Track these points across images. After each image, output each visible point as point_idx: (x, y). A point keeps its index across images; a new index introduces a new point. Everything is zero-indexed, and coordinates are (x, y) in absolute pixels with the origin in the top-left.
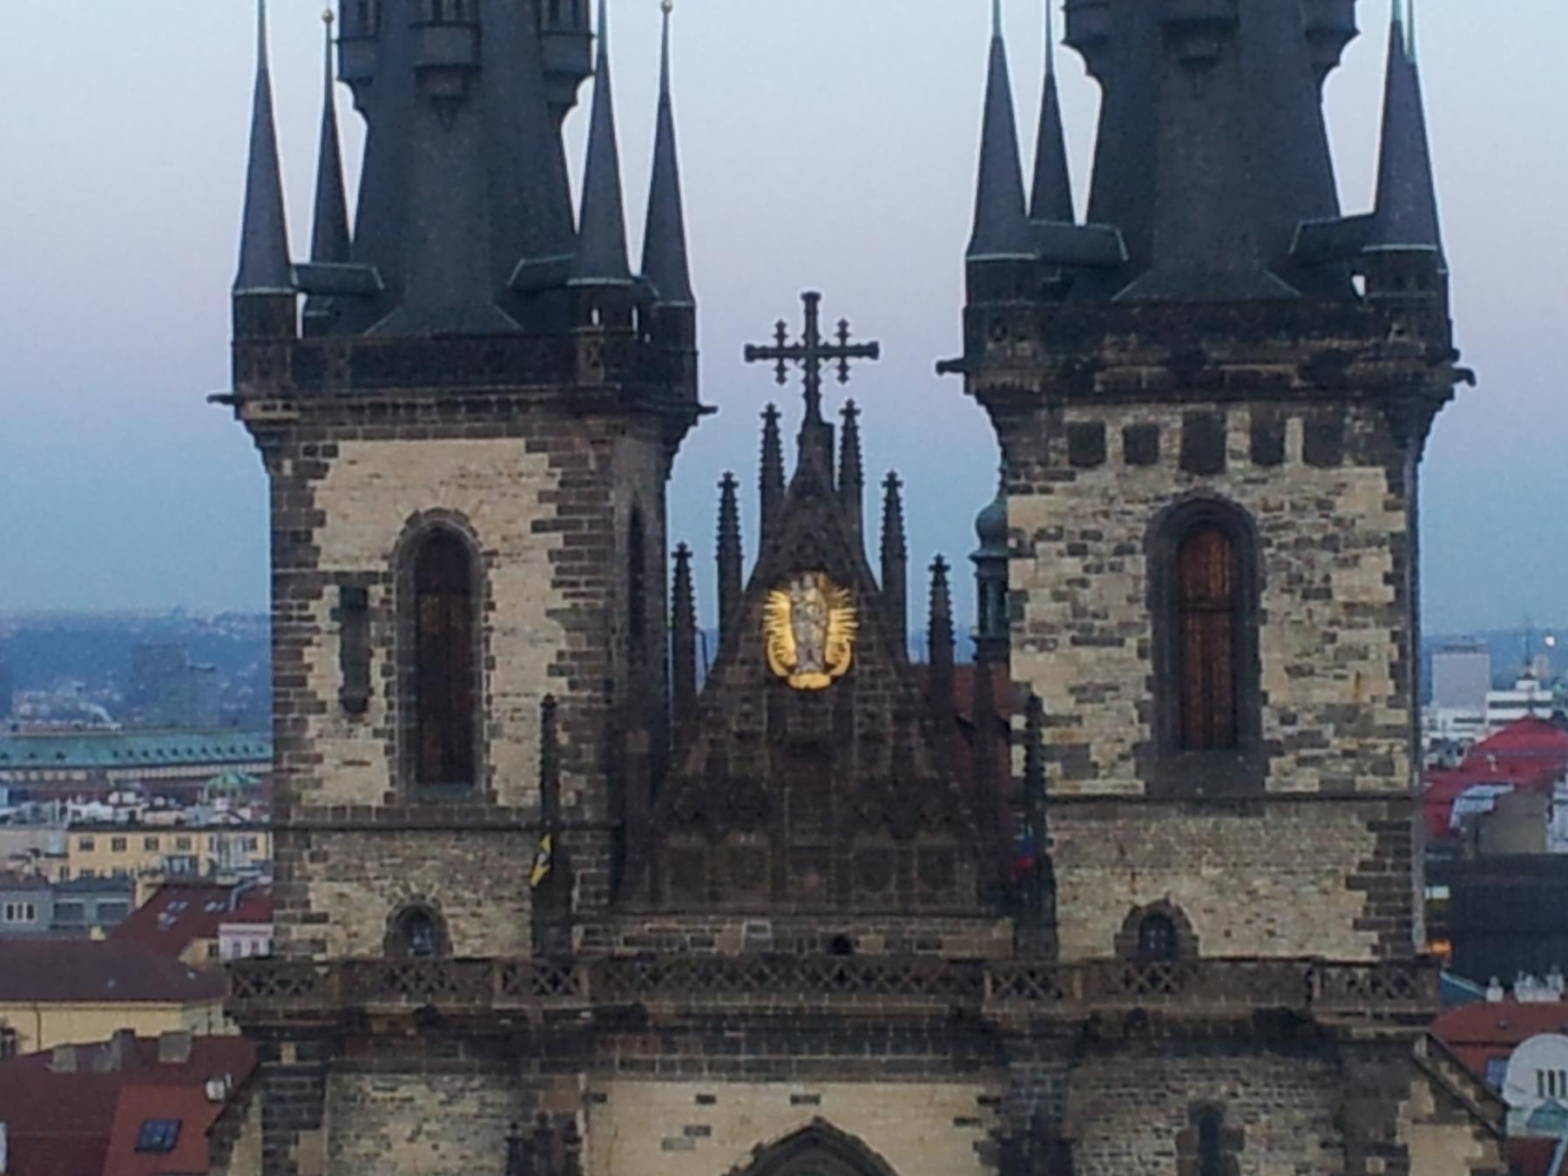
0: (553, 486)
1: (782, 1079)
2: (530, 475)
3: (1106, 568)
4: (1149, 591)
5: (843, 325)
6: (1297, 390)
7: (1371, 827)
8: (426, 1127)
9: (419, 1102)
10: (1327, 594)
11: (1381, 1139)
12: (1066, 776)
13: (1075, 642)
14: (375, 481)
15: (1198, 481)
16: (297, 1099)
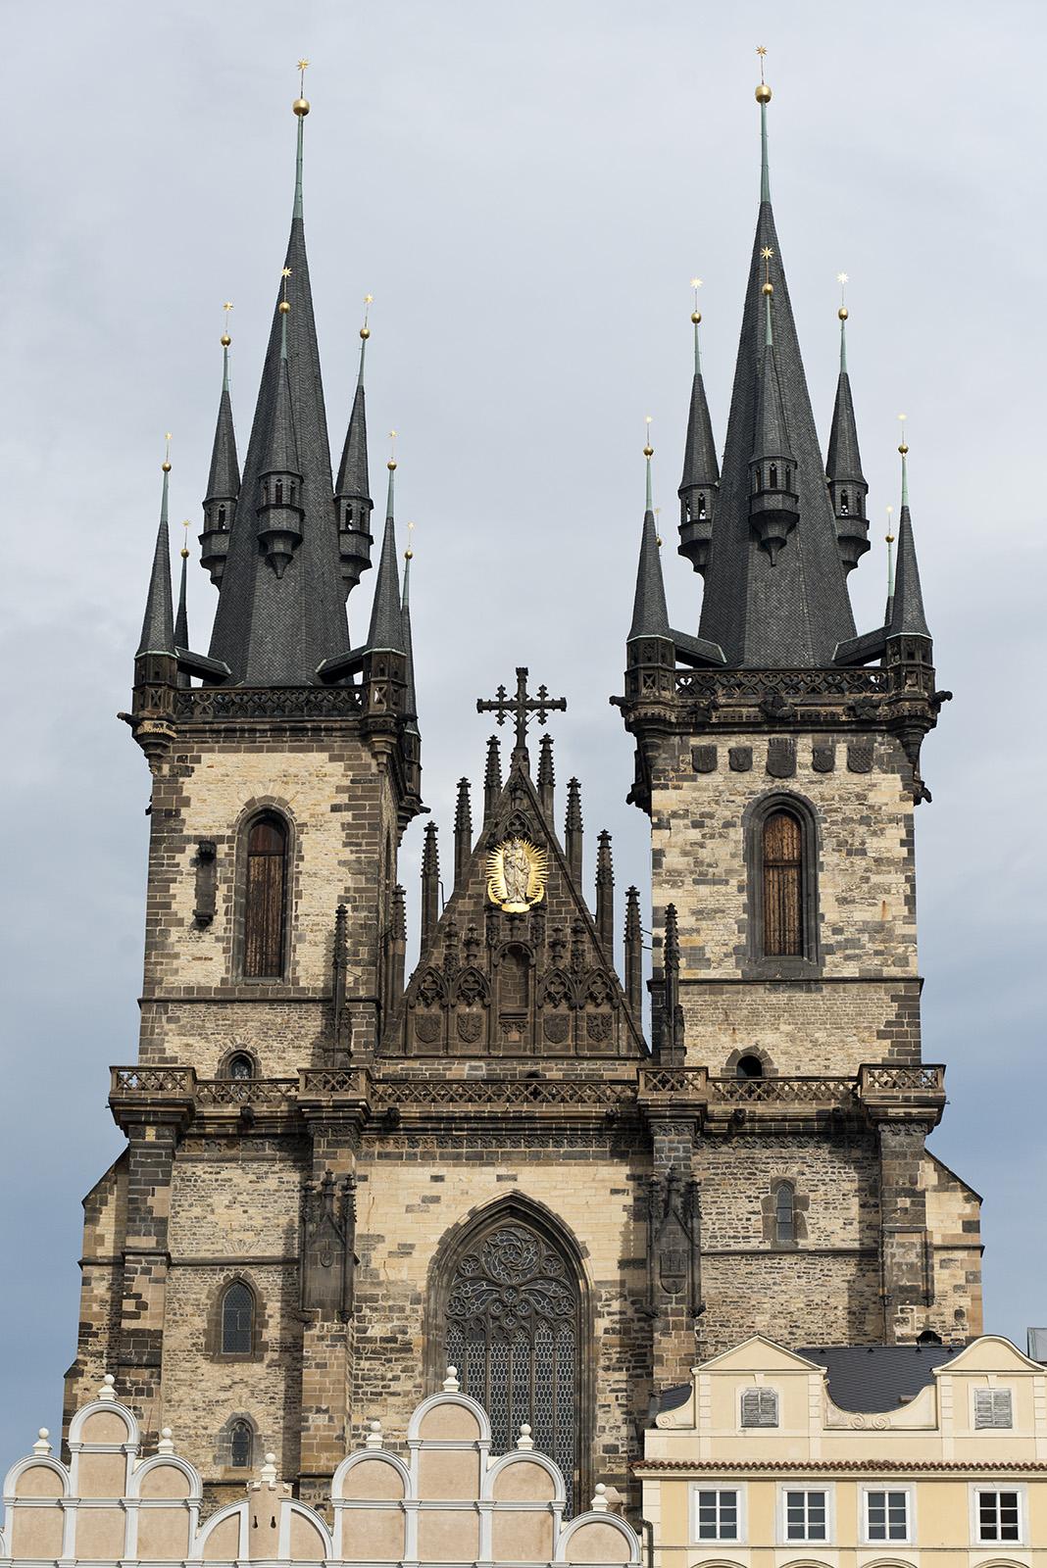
0: (347, 782)
1: (493, 1164)
2: (331, 776)
3: (717, 836)
4: (746, 852)
5: (543, 688)
6: (844, 723)
7: (894, 999)
8: (240, 1198)
10: (863, 852)
11: (907, 1185)
12: (689, 967)
13: (696, 882)
14: (226, 778)
15: (778, 782)
16: (158, 1164)
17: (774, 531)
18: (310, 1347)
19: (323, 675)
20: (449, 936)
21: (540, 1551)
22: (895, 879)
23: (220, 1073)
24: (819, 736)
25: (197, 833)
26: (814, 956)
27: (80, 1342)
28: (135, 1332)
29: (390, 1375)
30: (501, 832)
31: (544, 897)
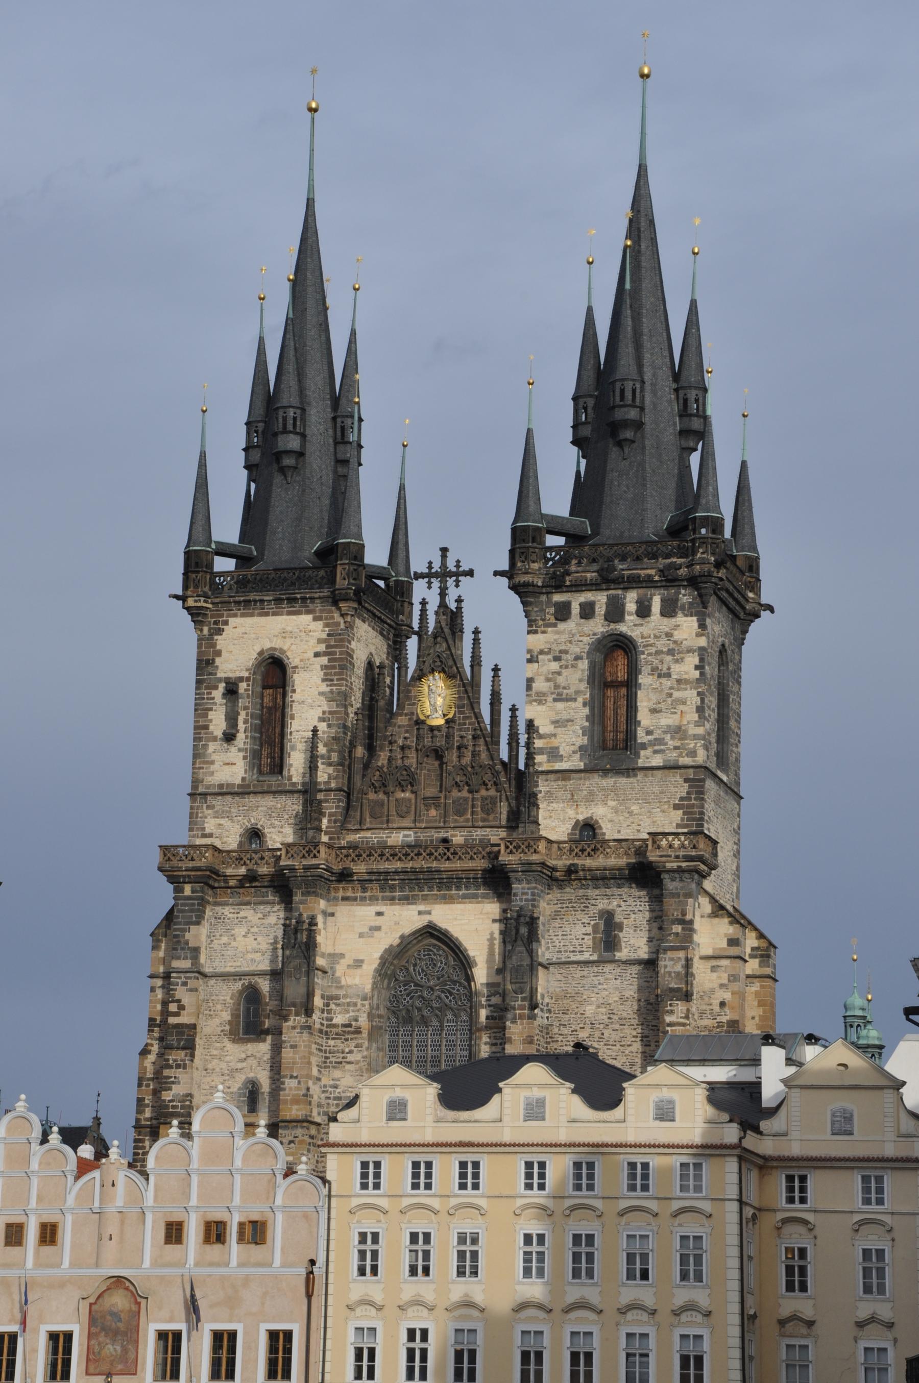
0: (324, 636)
2: (314, 631)
5: (458, 561)
7: (686, 781)
8: (252, 930)
9: (249, 918)
10: (668, 675)
11: (680, 917)
12: (549, 761)
13: (555, 700)
15: (613, 626)
16: (192, 911)
17: (628, 434)
18: (286, 1033)
19: (318, 553)
20: (391, 743)
21: (268, 1199)
22: (691, 696)
23: (241, 844)
24: (641, 591)
25: (226, 675)
26: (633, 751)
27: (149, 1031)
28: (177, 1026)
29: (347, 1050)
30: (426, 668)
31: (455, 714)
